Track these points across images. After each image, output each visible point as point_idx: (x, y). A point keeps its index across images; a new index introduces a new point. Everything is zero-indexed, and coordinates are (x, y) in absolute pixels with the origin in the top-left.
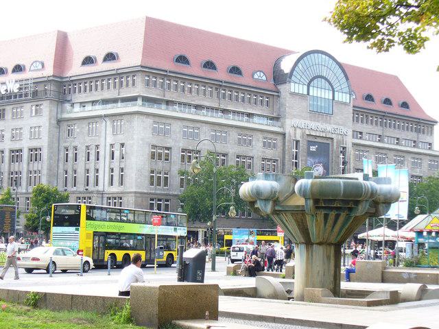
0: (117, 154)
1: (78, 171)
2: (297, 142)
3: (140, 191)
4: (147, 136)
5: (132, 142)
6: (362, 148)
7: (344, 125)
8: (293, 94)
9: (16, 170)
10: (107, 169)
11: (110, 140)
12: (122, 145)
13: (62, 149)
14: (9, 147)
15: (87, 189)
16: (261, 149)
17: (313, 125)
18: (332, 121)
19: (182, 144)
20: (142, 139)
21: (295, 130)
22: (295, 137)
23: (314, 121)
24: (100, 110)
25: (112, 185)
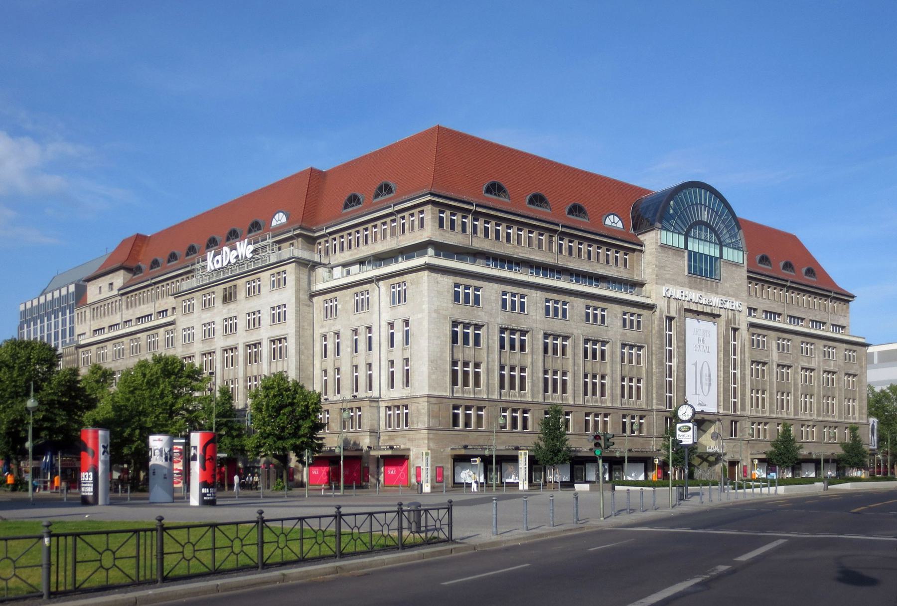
0: (399, 337)
1: (342, 369)
2: (670, 319)
3: (436, 393)
4: (445, 305)
5: (420, 316)
6: (759, 331)
7: (736, 296)
9: (255, 374)
10: (384, 363)
11: (386, 317)
12: (406, 322)
13: (317, 337)
14: (245, 341)
15: (354, 396)
16: (621, 330)
17: (694, 295)
18: (719, 290)
19: (502, 318)
20: (437, 311)
21: (669, 302)
22: (669, 312)
23: (695, 288)
24: (371, 272)
25: (392, 387)
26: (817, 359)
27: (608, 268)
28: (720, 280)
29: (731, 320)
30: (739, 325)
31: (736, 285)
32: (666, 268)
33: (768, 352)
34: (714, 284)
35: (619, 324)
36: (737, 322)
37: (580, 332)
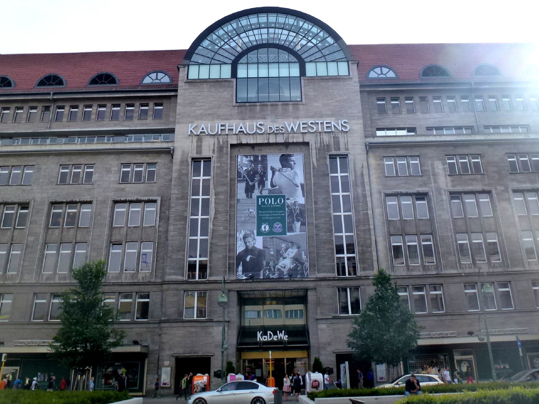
2: (208, 160)
6: (401, 152)
8: (191, 82)
23: (253, 118)
28: (301, 101)
29: (328, 146)
30: (347, 149)
31: (337, 101)
32: (197, 104)
33: (425, 178)
34: (291, 107)
35: (112, 179)
36: (342, 146)
37: (45, 195)
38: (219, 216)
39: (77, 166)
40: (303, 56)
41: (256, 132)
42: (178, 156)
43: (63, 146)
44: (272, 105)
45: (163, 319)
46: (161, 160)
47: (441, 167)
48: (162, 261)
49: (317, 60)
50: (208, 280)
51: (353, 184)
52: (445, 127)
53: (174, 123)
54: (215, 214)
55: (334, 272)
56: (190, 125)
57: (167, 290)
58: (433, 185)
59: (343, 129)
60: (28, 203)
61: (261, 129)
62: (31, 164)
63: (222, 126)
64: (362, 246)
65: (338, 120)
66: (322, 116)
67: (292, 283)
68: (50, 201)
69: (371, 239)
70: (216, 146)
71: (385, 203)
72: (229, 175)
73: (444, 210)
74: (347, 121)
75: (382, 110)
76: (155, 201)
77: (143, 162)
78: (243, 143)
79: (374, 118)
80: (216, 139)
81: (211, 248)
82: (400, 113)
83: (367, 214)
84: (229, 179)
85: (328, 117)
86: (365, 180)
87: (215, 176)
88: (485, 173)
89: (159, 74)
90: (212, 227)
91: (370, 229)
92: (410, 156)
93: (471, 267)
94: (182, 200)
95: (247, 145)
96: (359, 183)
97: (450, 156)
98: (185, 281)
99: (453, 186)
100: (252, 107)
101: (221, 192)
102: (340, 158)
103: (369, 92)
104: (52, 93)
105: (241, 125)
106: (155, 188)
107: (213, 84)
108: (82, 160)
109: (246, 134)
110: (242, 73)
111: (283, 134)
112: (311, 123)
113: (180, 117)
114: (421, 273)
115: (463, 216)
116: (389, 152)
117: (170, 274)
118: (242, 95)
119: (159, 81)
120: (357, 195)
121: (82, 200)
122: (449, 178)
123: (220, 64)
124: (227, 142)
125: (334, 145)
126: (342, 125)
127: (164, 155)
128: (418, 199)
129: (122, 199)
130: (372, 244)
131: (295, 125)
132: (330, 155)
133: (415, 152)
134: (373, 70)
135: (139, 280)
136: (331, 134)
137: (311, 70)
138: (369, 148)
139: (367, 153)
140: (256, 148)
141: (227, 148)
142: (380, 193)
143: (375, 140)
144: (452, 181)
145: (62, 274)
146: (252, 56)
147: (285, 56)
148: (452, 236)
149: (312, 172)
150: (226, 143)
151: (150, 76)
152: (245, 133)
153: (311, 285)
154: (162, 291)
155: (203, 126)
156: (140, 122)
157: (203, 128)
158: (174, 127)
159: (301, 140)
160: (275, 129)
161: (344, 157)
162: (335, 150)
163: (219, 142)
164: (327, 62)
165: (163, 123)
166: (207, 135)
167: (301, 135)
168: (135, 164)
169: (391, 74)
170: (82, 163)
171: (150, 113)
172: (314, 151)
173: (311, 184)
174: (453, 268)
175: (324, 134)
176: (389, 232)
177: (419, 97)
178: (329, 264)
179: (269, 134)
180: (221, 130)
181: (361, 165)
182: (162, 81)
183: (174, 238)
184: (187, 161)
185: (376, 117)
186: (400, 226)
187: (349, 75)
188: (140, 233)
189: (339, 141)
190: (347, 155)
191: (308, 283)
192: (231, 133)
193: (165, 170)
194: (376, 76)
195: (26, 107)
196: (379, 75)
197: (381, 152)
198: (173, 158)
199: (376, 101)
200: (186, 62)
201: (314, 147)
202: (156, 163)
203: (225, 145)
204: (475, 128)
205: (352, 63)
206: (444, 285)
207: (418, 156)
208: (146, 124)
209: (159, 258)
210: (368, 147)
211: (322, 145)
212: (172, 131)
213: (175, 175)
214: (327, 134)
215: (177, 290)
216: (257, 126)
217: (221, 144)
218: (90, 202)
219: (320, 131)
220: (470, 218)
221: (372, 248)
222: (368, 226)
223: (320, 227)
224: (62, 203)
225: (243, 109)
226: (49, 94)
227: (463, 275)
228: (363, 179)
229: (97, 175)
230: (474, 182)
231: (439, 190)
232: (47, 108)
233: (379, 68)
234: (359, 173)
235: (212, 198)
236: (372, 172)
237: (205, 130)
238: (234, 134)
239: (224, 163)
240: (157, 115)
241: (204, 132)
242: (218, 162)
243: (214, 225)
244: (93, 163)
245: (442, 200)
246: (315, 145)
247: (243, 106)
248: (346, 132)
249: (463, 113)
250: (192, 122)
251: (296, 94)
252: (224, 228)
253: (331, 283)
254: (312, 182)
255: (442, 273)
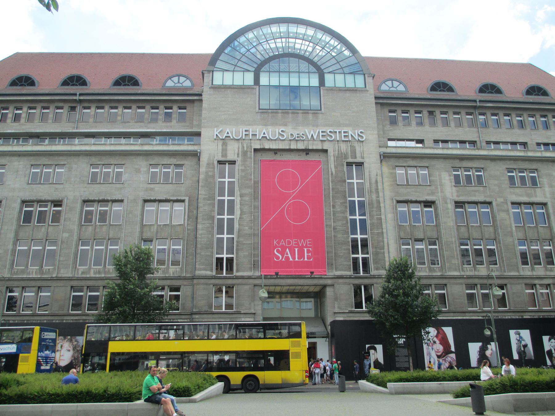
2: (233, 163)
21: (225, 144)
23: (274, 124)
26: (547, 189)
27: (152, 125)
28: (321, 110)
33: (433, 188)
34: (310, 116)
35: (142, 179)
36: (358, 155)
38: (244, 216)
39: (108, 165)
40: (322, 67)
41: (278, 138)
42: (204, 159)
43: (93, 146)
44: (293, 113)
45: (194, 310)
46: (188, 163)
47: (447, 178)
48: (191, 257)
49: (335, 72)
50: (235, 276)
51: (368, 190)
52: (450, 141)
53: (199, 126)
54: (241, 215)
55: (350, 271)
56: (215, 129)
57: (198, 284)
58: (440, 194)
59: (359, 138)
60: (61, 201)
61: (283, 136)
62: (62, 163)
63: (246, 131)
64: (376, 248)
65: (355, 130)
66: (339, 125)
67: (312, 280)
68: (83, 199)
69: (383, 242)
70: (240, 150)
71: (396, 209)
72: (253, 178)
73: (449, 217)
74: (363, 131)
75: (393, 122)
76: (183, 201)
77: (171, 163)
78: (266, 148)
79: (385, 129)
80: (240, 144)
81: (237, 246)
82: (409, 124)
83: (381, 219)
84: (253, 182)
85: (345, 127)
86: (379, 187)
87: (240, 178)
88: (487, 185)
89: (181, 77)
90: (238, 226)
91: (382, 233)
92: (420, 167)
93: (472, 270)
94: (209, 200)
95: (270, 150)
96: (373, 189)
97: (456, 169)
98: (213, 276)
99: (458, 196)
100: (274, 114)
101: (246, 194)
102: (355, 165)
103: (382, 104)
104: (78, 94)
105: (264, 131)
106: (183, 189)
107: (237, 90)
108: (113, 161)
109: (269, 140)
110: (264, 80)
111: (303, 140)
112: (330, 132)
113: (206, 121)
114: (427, 274)
115: (466, 224)
116: (402, 162)
117: (200, 269)
118: (264, 103)
119: (180, 85)
120: (372, 201)
121: (114, 199)
122: (454, 188)
123: (244, 71)
124: (251, 146)
125: (351, 153)
126: (358, 134)
127: (190, 157)
128: (425, 206)
129: (152, 198)
130: (385, 246)
131: (315, 133)
132: (347, 163)
133: (425, 163)
134: (384, 83)
135: (170, 275)
136: (349, 142)
137: (329, 80)
138: (383, 157)
139: (381, 162)
140: (279, 153)
141: (251, 152)
142: (392, 199)
143: (388, 150)
144: (458, 191)
145: (96, 269)
146: (274, 64)
147: (304, 66)
148: (455, 241)
149: (330, 177)
150: (249, 147)
151: (172, 79)
152: (268, 138)
153: (329, 282)
154: (193, 285)
155: (228, 130)
156: (164, 124)
157: (228, 132)
158: (199, 130)
159: (320, 147)
160: (296, 136)
161: (360, 165)
162: (352, 158)
163: (243, 147)
164: (344, 73)
165: (187, 126)
166: (232, 139)
167: (320, 143)
168: (163, 165)
169: (401, 88)
170: (112, 163)
171: (174, 116)
172: (332, 158)
173: (329, 189)
174: (455, 270)
175: (341, 142)
176: (399, 236)
177: (428, 111)
178: (345, 263)
179: (290, 140)
180: (245, 135)
181: (376, 173)
182: (184, 84)
183: (203, 236)
184: (213, 164)
185: (388, 127)
186: (409, 231)
187: (366, 87)
188: (170, 231)
189: (355, 150)
190: (363, 163)
191: (327, 280)
192: (254, 138)
193: (192, 172)
194: (387, 88)
195: (52, 107)
196: (390, 88)
197: (393, 162)
198: (199, 160)
199: (388, 112)
200: (211, 68)
201: (332, 154)
202: (183, 165)
203: (249, 150)
204: (478, 143)
205: (368, 77)
206: (448, 285)
207: (427, 167)
208: (171, 127)
209: (188, 254)
210: (382, 156)
211: (340, 152)
212: (198, 134)
213: (202, 177)
214: (344, 142)
215: (207, 284)
216: (279, 133)
217: (245, 149)
218: (122, 201)
219: (338, 139)
220: (472, 226)
221: (385, 250)
222: (381, 229)
223: (338, 229)
224: (94, 201)
225: (266, 115)
226: (76, 95)
227: (465, 277)
228: (377, 186)
229: (127, 175)
230: (477, 194)
231: (445, 199)
232: (73, 109)
233: (391, 82)
234: (373, 181)
235: (237, 199)
236: (385, 179)
237: (230, 135)
238: (258, 140)
239: (248, 167)
240: (182, 119)
241: (229, 137)
242: (242, 165)
243: (239, 225)
244: (123, 163)
245: (448, 209)
246: (333, 153)
247: (266, 113)
248: (362, 142)
249: (468, 129)
250: (217, 126)
251: (315, 103)
252: (249, 228)
253: (347, 281)
254: (331, 187)
255: (446, 274)
